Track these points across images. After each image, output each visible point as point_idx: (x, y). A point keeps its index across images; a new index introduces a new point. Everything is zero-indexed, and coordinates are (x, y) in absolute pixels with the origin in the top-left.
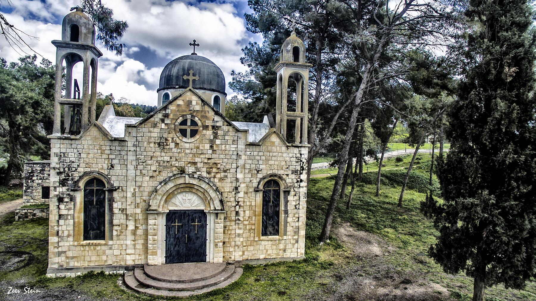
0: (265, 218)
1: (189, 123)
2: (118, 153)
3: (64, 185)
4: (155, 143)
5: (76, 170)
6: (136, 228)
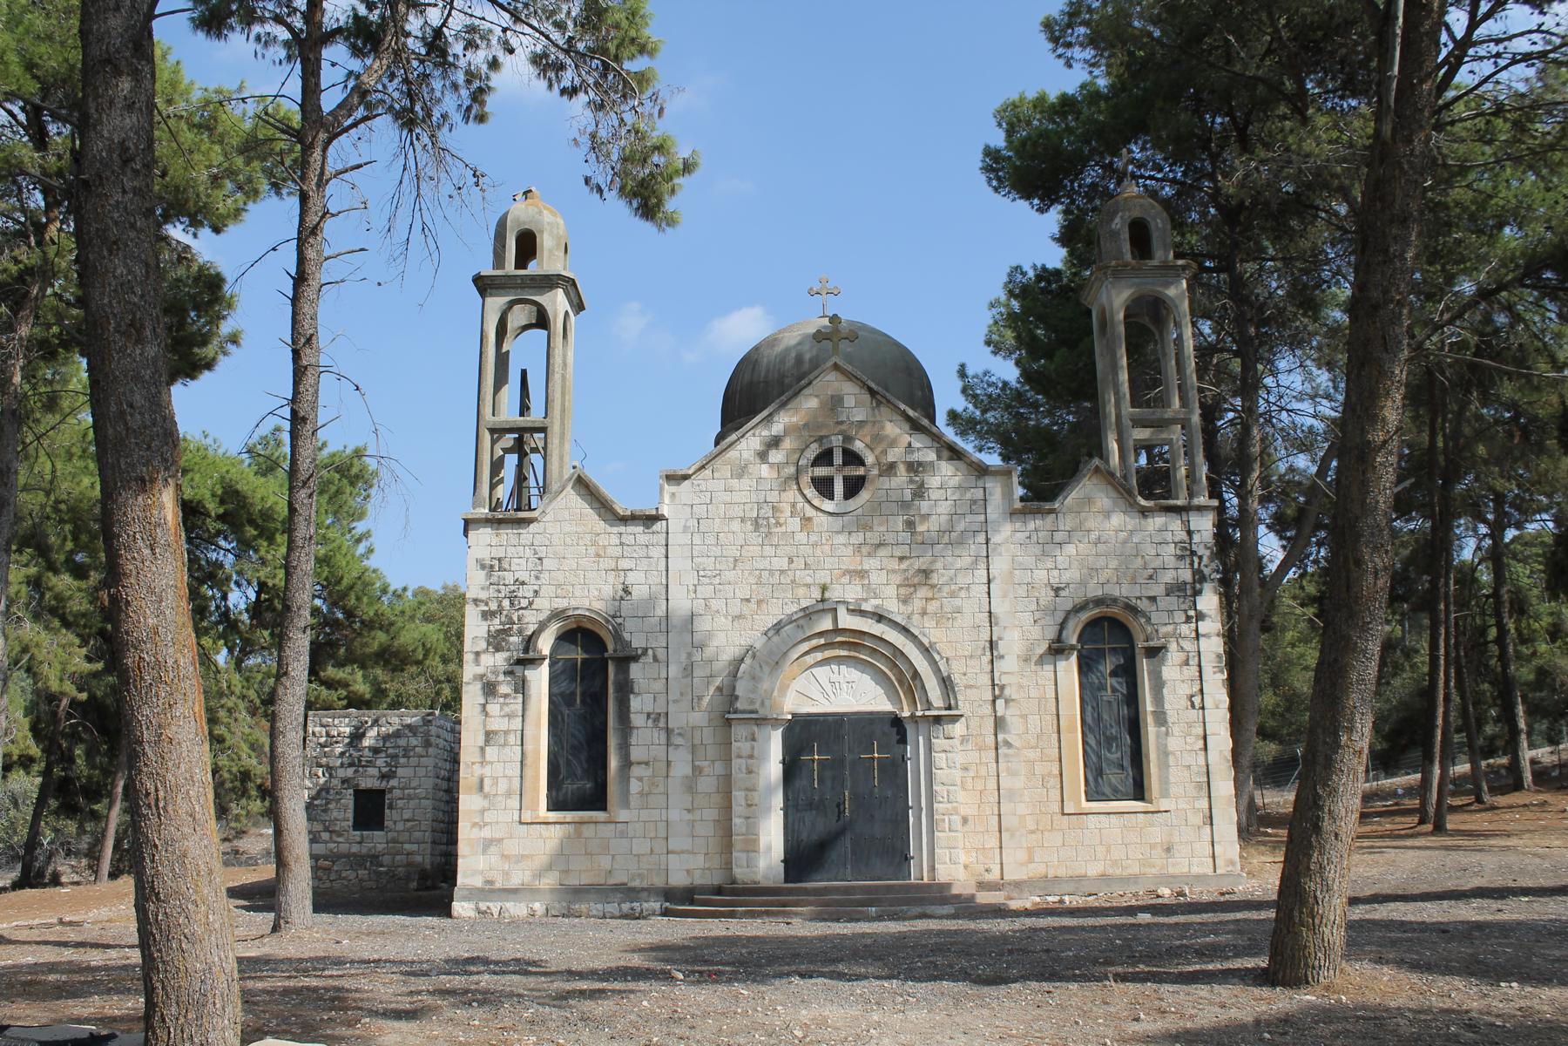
0: (1092, 742)
1: (838, 459)
2: (642, 553)
3: (498, 649)
4: (743, 520)
5: (531, 604)
6: (697, 771)
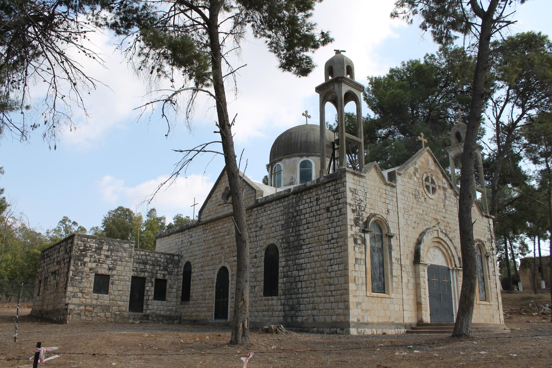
5: (364, 209)
